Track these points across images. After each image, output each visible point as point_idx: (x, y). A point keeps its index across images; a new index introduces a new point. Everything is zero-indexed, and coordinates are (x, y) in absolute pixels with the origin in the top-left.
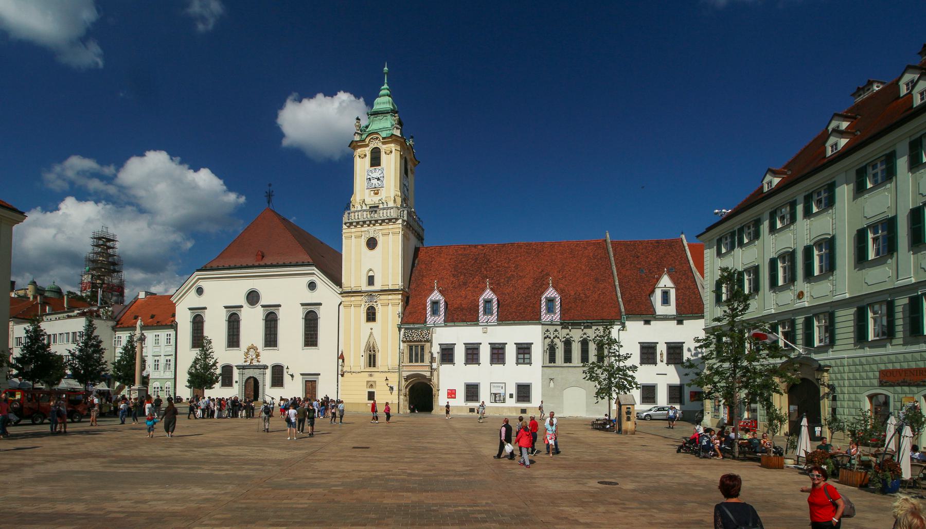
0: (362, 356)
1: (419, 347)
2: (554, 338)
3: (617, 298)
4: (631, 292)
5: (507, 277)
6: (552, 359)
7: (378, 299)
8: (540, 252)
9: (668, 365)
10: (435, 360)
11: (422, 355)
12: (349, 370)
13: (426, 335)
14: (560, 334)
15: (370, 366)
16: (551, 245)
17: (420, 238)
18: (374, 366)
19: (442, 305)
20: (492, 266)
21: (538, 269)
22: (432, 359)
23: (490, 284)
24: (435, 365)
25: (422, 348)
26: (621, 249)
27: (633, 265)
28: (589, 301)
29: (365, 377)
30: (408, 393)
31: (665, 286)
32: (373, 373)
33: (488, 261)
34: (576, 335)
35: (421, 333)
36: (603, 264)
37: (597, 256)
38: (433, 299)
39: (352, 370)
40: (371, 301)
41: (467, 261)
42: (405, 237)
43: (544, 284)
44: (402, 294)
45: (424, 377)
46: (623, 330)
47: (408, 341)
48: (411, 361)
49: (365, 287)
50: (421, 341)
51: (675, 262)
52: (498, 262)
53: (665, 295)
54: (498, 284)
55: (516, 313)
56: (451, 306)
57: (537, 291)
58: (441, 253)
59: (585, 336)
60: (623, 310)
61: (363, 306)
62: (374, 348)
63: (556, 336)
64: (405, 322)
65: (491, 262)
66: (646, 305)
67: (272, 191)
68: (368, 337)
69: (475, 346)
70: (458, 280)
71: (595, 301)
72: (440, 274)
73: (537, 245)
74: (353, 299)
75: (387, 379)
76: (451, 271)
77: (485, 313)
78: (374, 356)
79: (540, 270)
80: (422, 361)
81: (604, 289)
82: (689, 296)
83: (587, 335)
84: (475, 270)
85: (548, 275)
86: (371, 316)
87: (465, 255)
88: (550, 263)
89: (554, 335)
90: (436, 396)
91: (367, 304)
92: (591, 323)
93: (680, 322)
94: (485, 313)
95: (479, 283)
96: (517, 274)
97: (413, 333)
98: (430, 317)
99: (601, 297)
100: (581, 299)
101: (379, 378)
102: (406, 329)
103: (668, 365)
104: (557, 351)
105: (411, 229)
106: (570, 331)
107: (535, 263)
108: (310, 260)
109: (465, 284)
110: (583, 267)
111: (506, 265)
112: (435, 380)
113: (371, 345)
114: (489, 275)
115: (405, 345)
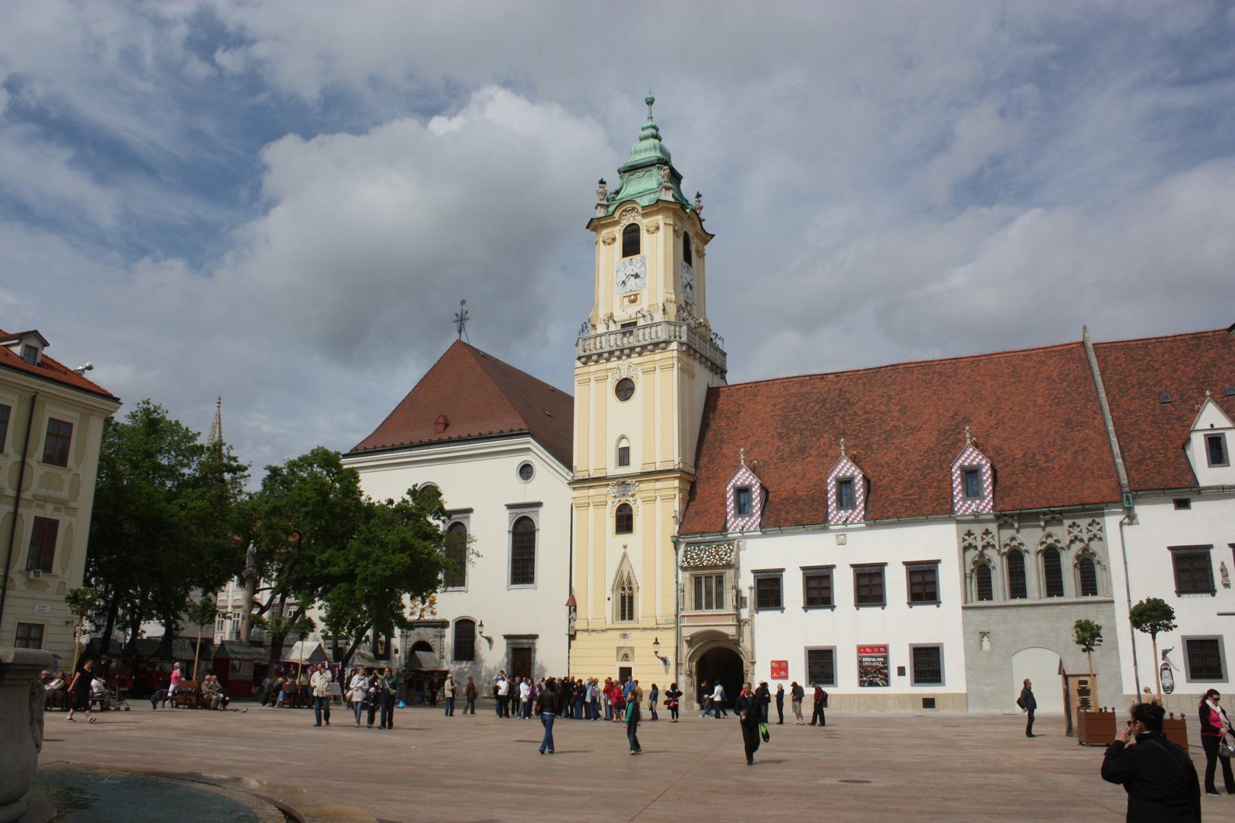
0: (609, 599)
3: (1113, 457)
4: (1143, 443)
5: (885, 432)
6: (985, 591)
7: (637, 489)
8: (950, 377)
10: (745, 603)
11: (720, 596)
12: (585, 627)
13: (726, 555)
14: (996, 538)
15: (623, 618)
16: (972, 362)
18: (631, 617)
20: (855, 412)
21: (948, 410)
22: (740, 602)
24: (745, 613)
26: (1117, 358)
28: (1053, 468)
29: (614, 639)
30: (694, 669)
31: (1212, 426)
32: (628, 632)
33: (848, 402)
34: (1031, 539)
35: (717, 552)
36: (1080, 390)
37: (1067, 375)
39: (591, 627)
40: (624, 495)
41: (807, 405)
42: (685, 371)
44: (679, 478)
45: (724, 636)
46: (1130, 524)
47: (692, 567)
48: (698, 606)
49: (613, 469)
50: (716, 566)
52: (866, 403)
55: (902, 501)
56: (775, 497)
57: (946, 454)
58: (756, 395)
59: (1050, 541)
60: (1124, 481)
62: (630, 582)
64: (686, 531)
65: (853, 404)
67: (467, 312)
69: (824, 572)
70: (790, 444)
71: (1067, 469)
72: (754, 434)
73: (944, 364)
74: (592, 492)
75: (656, 643)
76: (776, 428)
77: (841, 505)
78: (631, 598)
79: (951, 414)
80: (720, 605)
81: (1085, 440)
83: (1055, 538)
84: (822, 424)
85: (967, 420)
86: (624, 522)
88: (971, 398)
89: (984, 543)
90: (750, 675)
91: (618, 499)
92: (1061, 512)
94: (841, 505)
95: (830, 447)
96: (904, 424)
97: (701, 551)
98: (733, 520)
99: (1080, 458)
100: (1036, 466)
101: (640, 642)
102: (688, 544)
108: (524, 427)
109: (802, 450)
110: (1040, 401)
111: (883, 408)
112: (745, 644)
113: (625, 578)
115: (687, 574)
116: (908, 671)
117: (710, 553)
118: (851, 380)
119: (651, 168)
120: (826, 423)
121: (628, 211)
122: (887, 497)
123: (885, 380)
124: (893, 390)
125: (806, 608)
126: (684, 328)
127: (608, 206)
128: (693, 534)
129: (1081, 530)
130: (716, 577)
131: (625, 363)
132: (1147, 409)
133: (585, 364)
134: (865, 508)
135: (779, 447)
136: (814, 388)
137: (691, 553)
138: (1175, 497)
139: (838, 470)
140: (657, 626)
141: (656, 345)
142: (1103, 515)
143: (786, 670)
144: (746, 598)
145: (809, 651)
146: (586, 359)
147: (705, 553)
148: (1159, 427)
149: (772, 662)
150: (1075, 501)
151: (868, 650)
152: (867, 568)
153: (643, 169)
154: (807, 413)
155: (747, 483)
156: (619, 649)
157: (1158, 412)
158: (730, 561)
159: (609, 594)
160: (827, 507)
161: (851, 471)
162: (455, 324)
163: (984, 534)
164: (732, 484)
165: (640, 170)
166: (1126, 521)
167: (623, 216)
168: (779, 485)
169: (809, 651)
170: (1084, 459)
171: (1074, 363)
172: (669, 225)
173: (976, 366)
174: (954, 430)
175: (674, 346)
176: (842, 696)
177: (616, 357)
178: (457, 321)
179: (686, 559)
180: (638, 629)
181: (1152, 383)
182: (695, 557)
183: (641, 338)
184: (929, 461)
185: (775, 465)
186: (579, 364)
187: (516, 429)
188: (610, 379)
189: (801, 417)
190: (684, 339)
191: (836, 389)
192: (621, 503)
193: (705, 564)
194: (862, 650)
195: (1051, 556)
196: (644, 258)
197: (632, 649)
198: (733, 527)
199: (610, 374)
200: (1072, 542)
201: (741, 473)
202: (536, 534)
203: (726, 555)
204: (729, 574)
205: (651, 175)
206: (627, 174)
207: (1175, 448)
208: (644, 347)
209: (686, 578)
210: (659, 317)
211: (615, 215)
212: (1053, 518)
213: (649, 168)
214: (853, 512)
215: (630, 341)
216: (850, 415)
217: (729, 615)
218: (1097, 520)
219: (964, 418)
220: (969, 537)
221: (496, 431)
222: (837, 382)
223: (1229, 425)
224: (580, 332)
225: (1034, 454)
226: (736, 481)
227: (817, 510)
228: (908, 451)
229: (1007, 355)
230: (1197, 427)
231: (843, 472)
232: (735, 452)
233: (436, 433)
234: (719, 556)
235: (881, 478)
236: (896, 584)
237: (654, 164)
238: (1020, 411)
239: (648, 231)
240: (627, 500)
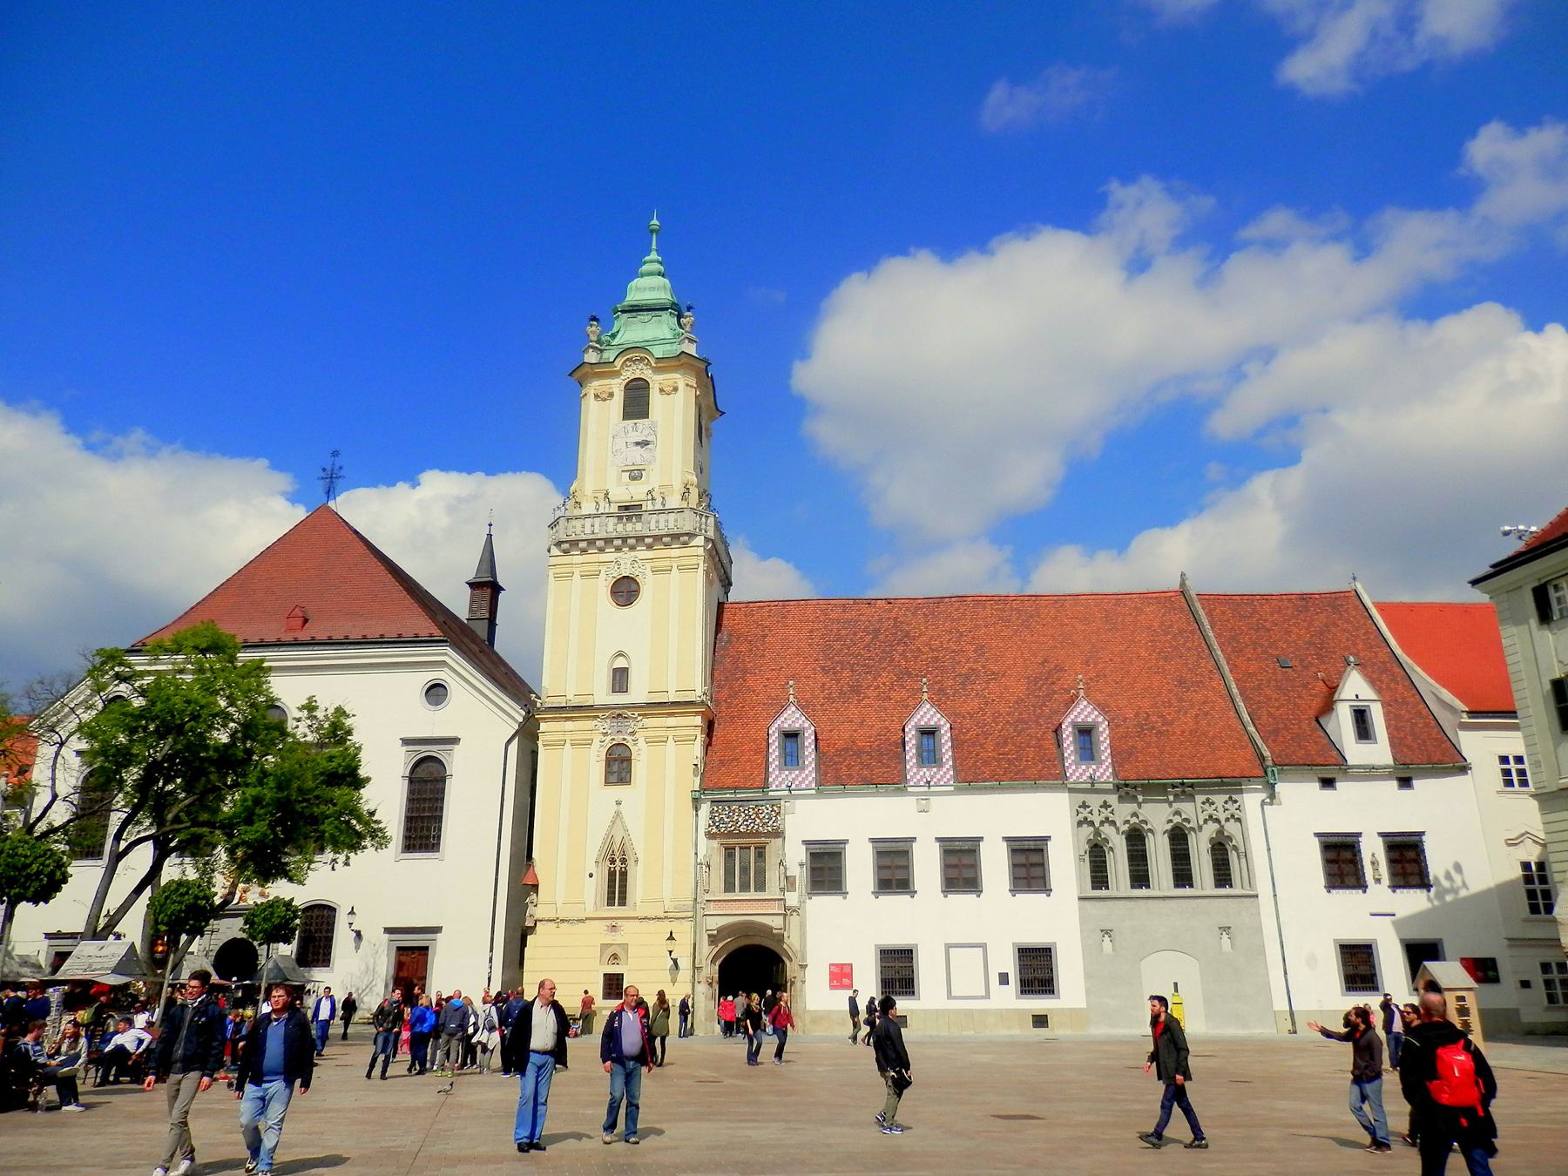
0: (591, 876)
1: (753, 848)
2: (1102, 823)
4: (1273, 711)
5: (960, 675)
6: (1099, 877)
7: (640, 725)
8: (1031, 616)
9: (1394, 892)
15: (611, 902)
16: (1056, 601)
17: (727, 583)
19: (809, 740)
25: (761, 853)
26: (1223, 613)
27: (1259, 650)
29: (597, 934)
32: (620, 923)
33: (907, 635)
34: (1158, 816)
37: (1171, 626)
38: (786, 725)
41: (855, 634)
43: (1055, 692)
45: (767, 930)
46: (1271, 804)
48: (729, 887)
49: (602, 694)
50: (758, 834)
51: (1355, 644)
53: (1361, 717)
54: (940, 689)
55: (998, 760)
59: (1177, 819)
61: (596, 743)
63: (1107, 818)
66: (1316, 743)
67: (341, 468)
68: (609, 823)
70: (838, 681)
71: (1191, 735)
74: (569, 725)
75: (671, 938)
78: (624, 874)
80: (761, 886)
81: (1205, 702)
82: (1409, 720)
86: (618, 767)
87: (847, 621)
88: (1061, 643)
89: (1102, 818)
90: (798, 984)
91: (610, 738)
92: (1192, 786)
93: (1405, 782)
96: (983, 667)
98: (777, 773)
103: (1394, 892)
104: (1109, 858)
106: (1140, 807)
107: (1024, 641)
108: (437, 632)
109: (856, 690)
113: (616, 847)
114: (914, 669)
115: (715, 843)
118: (907, 609)
119: (661, 313)
120: (882, 659)
121: (634, 362)
122: (977, 755)
123: (951, 613)
124: (964, 625)
125: (876, 894)
126: (711, 520)
127: (602, 351)
128: (722, 789)
129: (1092, 810)
131: (626, 556)
132: (1267, 672)
133: (566, 552)
134: (954, 767)
135: (824, 684)
136: (861, 615)
138: (1320, 776)
139: (919, 717)
140: (666, 915)
141: (675, 537)
142: (1241, 792)
143: (850, 976)
146: (569, 546)
148: (1285, 695)
149: (831, 965)
150: (1209, 772)
152: (957, 843)
154: (855, 644)
155: (797, 725)
156: (604, 946)
157: (1280, 677)
159: (592, 868)
160: (905, 762)
161: (935, 719)
163: (1101, 807)
164: (776, 726)
165: (645, 313)
166: (1268, 800)
167: (627, 366)
168: (831, 731)
170: (1209, 724)
171: (1176, 614)
172: (692, 387)
173: (1061, 606)
174: (1047, 679)
175: (700, 540)
176: (926, 1012)
177: (614, 547)
180: (637, 918)
181: (1266, 644)
182: (726, 820)
183: (653, 526)
184: (1021, 714)
185: (822, 705)
186: (555, 551)
187: (424, 634)
189: (848, 649)
190: (711, 534)
191: (889, 619)
192: (614, 742)
195: (1178, 837)
196: (654, 424)
197: (625, 946)
198: (777, 783)
199: (603, 569)
200: (1206, 821)
201: (789, 712)
204: (774, 844)
207: (1307, 719)
208: (658, 538)
209: (713, 848)
210: (674, 501)
211: (616, 363)
212: (1184, 792)
213: (657, 313)
215: (632, 528)
216: (912, 651)
218: (1234, 797)
219: (1056, 666)
221: (391, 634)
222: (890, 611)
223: (1373, 696)
224: (554, 510)
225: (1148, 715)
227: (889, 766)
229: (1096, 597)
230: (1341, 698)
231: (925, 720)
232: (765, 686)
233: (290, 629)
235: (964, 730)
236: (995, 865)
237: (667, 309)
238: (1122, 663)
239: (661, 390)
240: (624, 739)
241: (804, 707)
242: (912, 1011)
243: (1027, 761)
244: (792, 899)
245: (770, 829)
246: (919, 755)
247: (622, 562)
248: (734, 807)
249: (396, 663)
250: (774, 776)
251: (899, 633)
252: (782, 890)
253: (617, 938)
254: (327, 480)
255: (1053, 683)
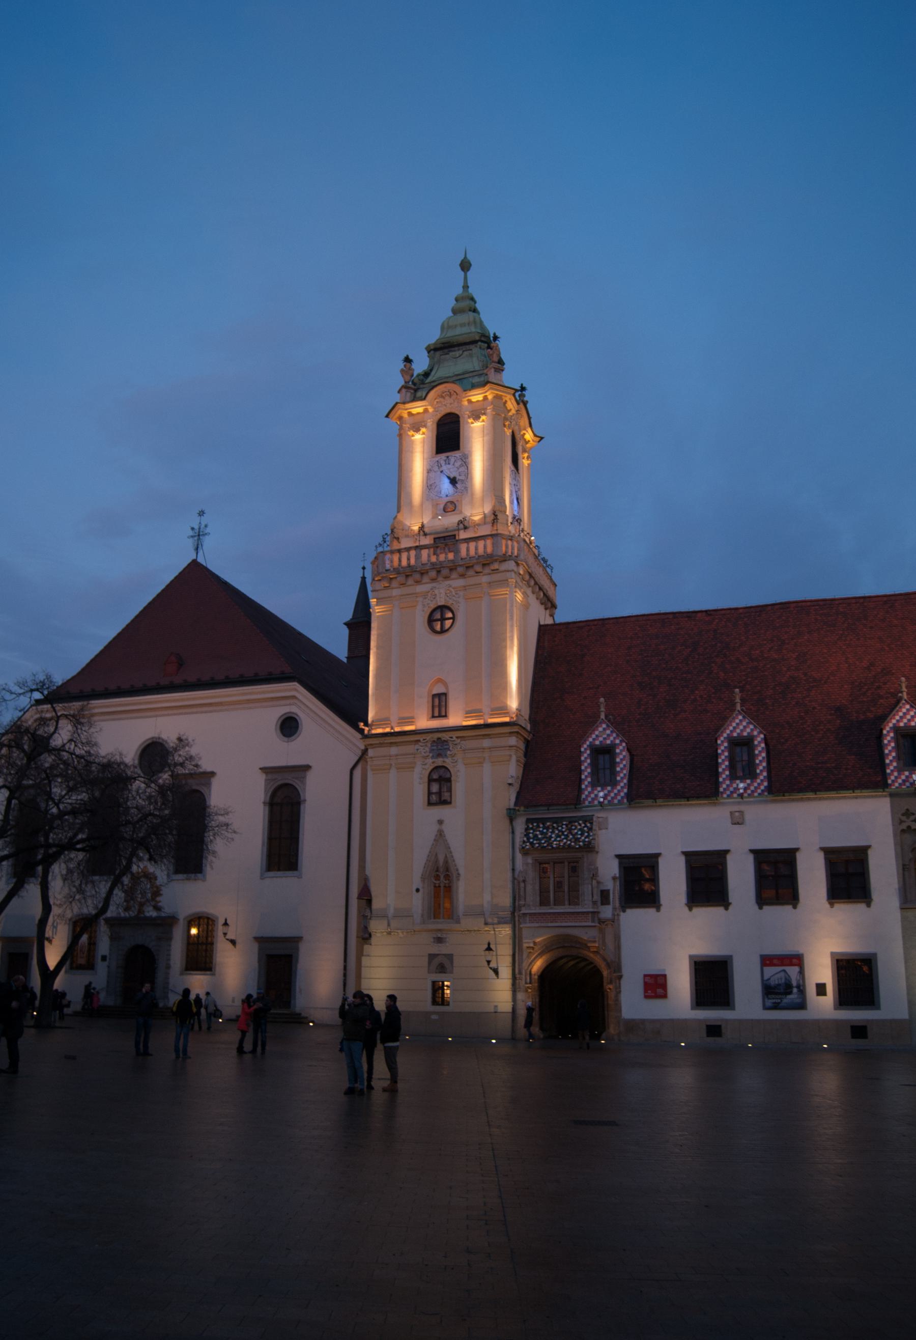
13: (582, 835)
23: (743, 701)
25: (574, 869)
35: (570, 830)
38: (597, 743)
40: (439, 755)
48: (544, 902)
62: (447, 869)
67: (206, 526)
75: (489, 949)
80: (574, 899)
97: (548, 828)
98: (589, 789)
105: (532, 583)
116: (830, 989)
117: (559, 831)
119: (471, 347)
130: (569, 863)
137: (534, 831)
144: (608, 891)
145: (695, 963)
147: (553, 832)
149: (645, 976)
151: (775, 961)
153: (461, 347)
155: (608, 742)
156: (432, 957)
158: (590, 842)
159: (417, 882)
160: (717, 775)
161: (748, 730)
162: (191, 540)
164: (588, 743)
165: (456, 348)
169: (695, 963)
176: (741, 1022)
178: (192, 537)
179: (528, 839)
182: (540, 836)
188: (419, 607)
192: (436, 765)
193: (555, 846)
194: (767, 961)
197: (450, 957)
201: (600, 729)
202: (302, 807)
203: (582, 835)
205: (471, 356)
206: (438, 353)
214: (752, 782)
217: (588, 913)
220: (908, 818)
224: (376, 547)
226: (594, 739)
228: (814, 708)
231: (738, 731)
234: (574, 835)
235: (782, 740)
241: (617, 725)
242: (727, 1021)
243: (847, 769)
244: (607, 912)
245: (581, 843)
246: (732, 767)
247: (436, 592)
248: (548, 824)
249: (259, 699)
250: (586, 793)
251: (719, 645)
252: (594, 903)
253: (444, 949)
254: (196, 538)
255: (879, 687)
